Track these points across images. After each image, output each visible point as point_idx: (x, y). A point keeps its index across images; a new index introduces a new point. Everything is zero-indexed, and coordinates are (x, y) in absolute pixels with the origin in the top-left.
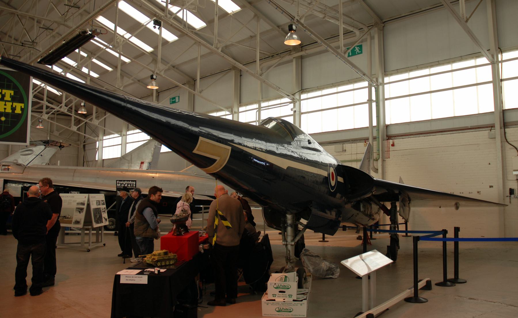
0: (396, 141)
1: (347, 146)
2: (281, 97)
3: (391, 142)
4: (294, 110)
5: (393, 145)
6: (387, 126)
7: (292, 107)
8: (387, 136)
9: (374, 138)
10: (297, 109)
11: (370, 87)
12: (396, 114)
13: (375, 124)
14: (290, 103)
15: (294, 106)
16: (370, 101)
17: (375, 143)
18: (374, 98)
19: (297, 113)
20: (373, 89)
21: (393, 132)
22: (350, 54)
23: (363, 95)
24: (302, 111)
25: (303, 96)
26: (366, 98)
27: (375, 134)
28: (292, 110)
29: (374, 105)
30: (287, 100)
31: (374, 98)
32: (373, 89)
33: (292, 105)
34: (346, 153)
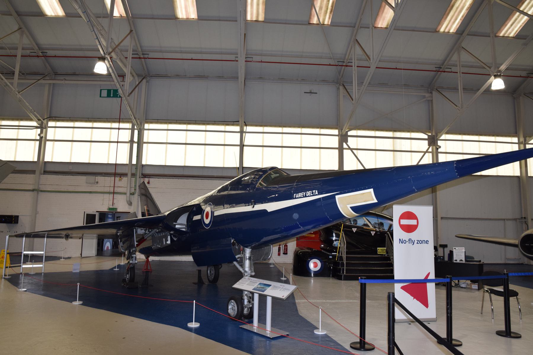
0: (152, 180)
1: (100, 179)
2: (31, 120)
3: (146, 180)
4: (42, 135)
5: (148, 183)
6: (143, 166)
7: (39, 133)
8: (142, 174)
9: (133, 175)
10: (43, 135)
11: (133, 130)
12: (153, 156)
13: (134, 162)
14: (37, 127)
15: (42, 132)
16: (132, 142)
17: (133, 179)
18: (136, 139)
19: (43, 139)
20: (136, 132)
21: (147, 171)
22: (112, 96)
23: (125, 135)
24: (48, 138)
25: (51, 124)
26: (128, 139)
27: (134, 172)
28: (39, 135)
29: (135, 146)
30: (34, 124)
31: (136, 139)
32: (136, 132)
33: (39, 131)
34: (98, 185)
